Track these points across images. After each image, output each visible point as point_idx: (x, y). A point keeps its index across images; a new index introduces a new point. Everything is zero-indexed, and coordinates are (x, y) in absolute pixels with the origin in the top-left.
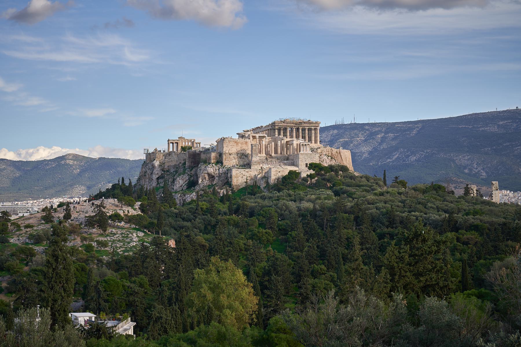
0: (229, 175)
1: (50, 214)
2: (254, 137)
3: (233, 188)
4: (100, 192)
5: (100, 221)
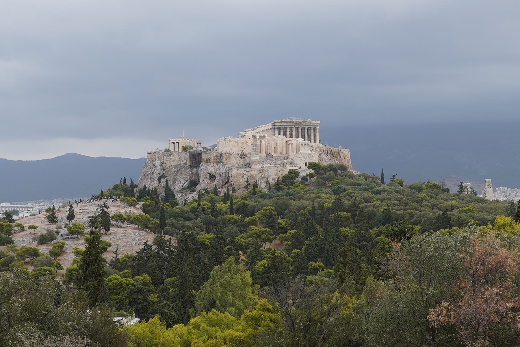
0: (230, 175)
1: (53, 214)
2: (254, 137)
4: (102, 192)
5: (103, 221)
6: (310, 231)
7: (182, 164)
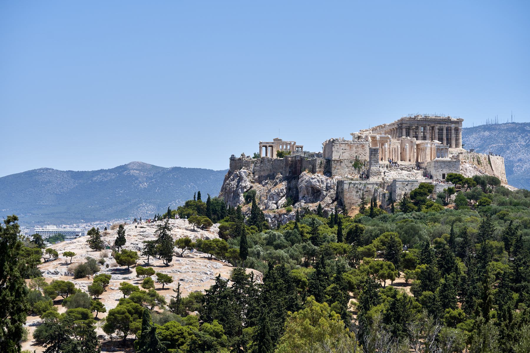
2: (373, 138)
3: (345, 206)
5: (163, 248)
6: (447, 266)
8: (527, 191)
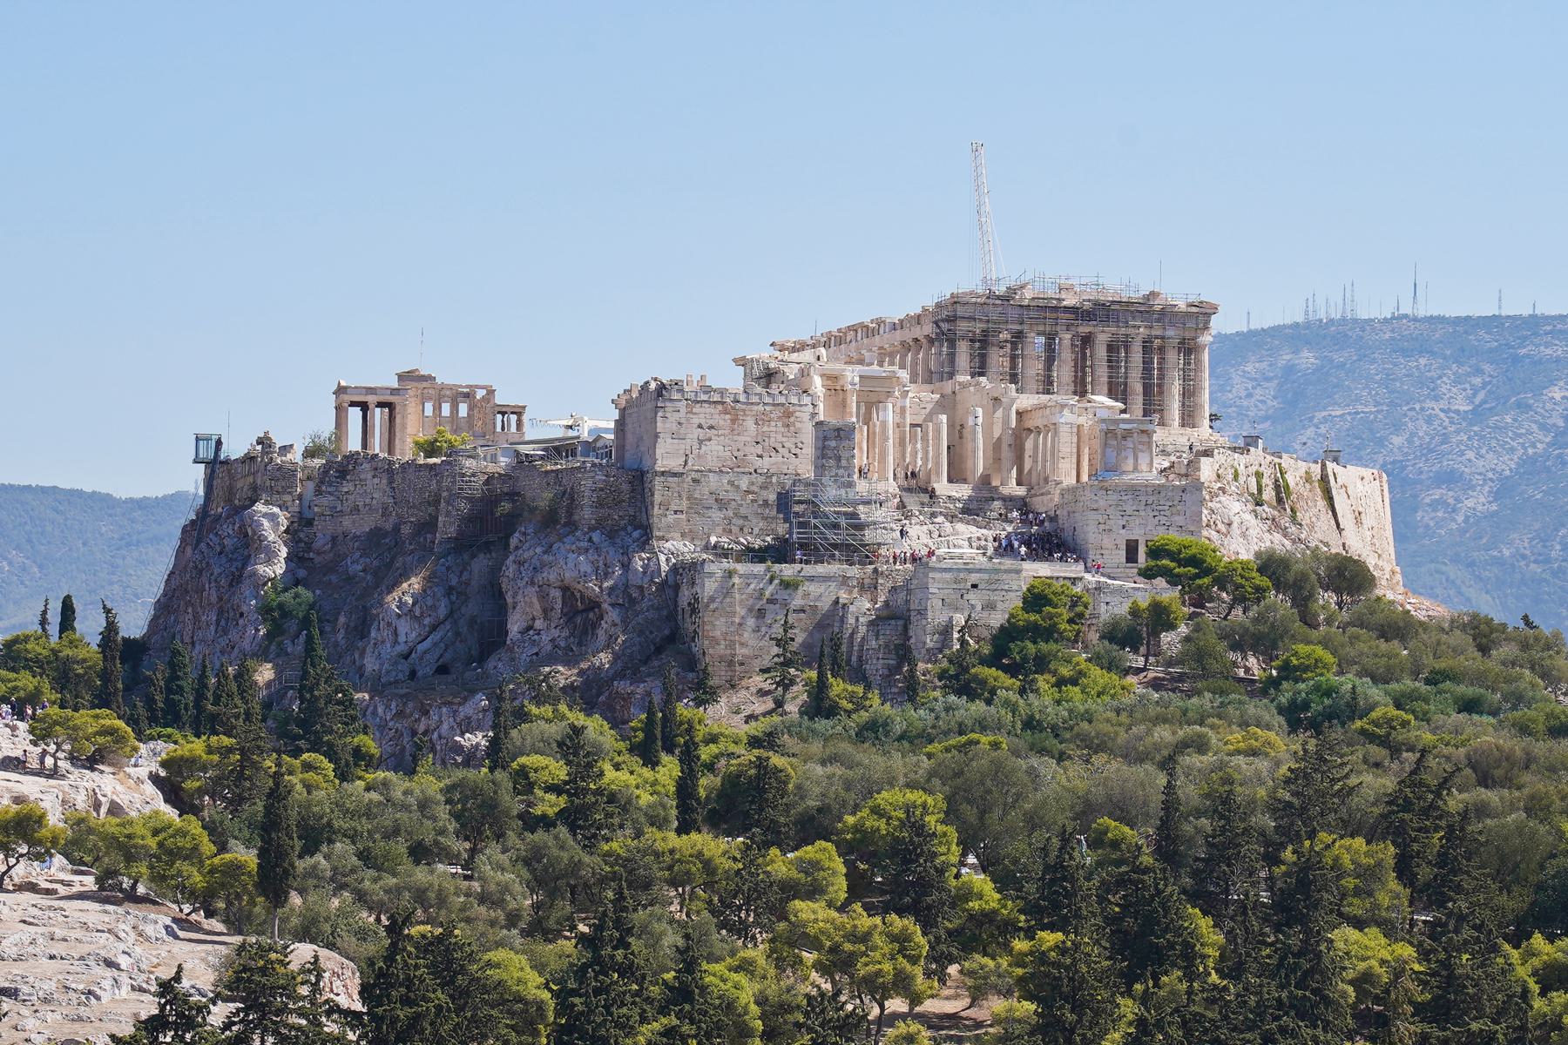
2: (834, 384)
7: (406, 530)
8: (1489, 622)
